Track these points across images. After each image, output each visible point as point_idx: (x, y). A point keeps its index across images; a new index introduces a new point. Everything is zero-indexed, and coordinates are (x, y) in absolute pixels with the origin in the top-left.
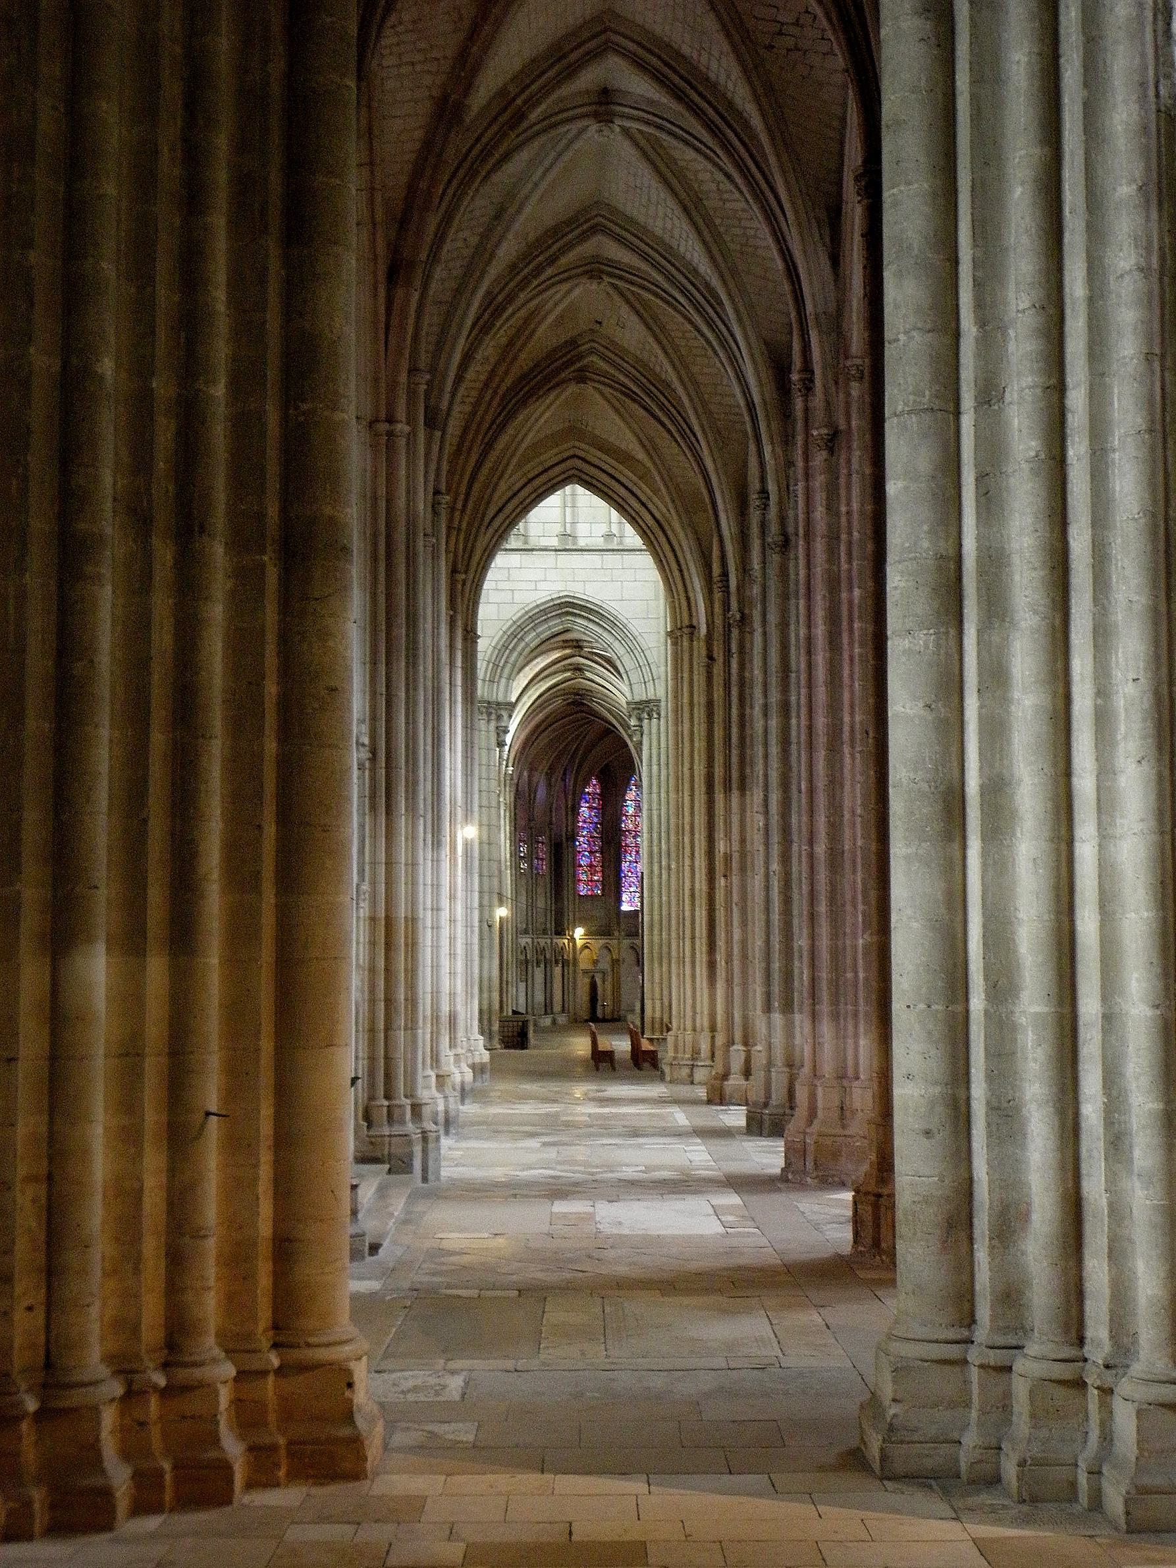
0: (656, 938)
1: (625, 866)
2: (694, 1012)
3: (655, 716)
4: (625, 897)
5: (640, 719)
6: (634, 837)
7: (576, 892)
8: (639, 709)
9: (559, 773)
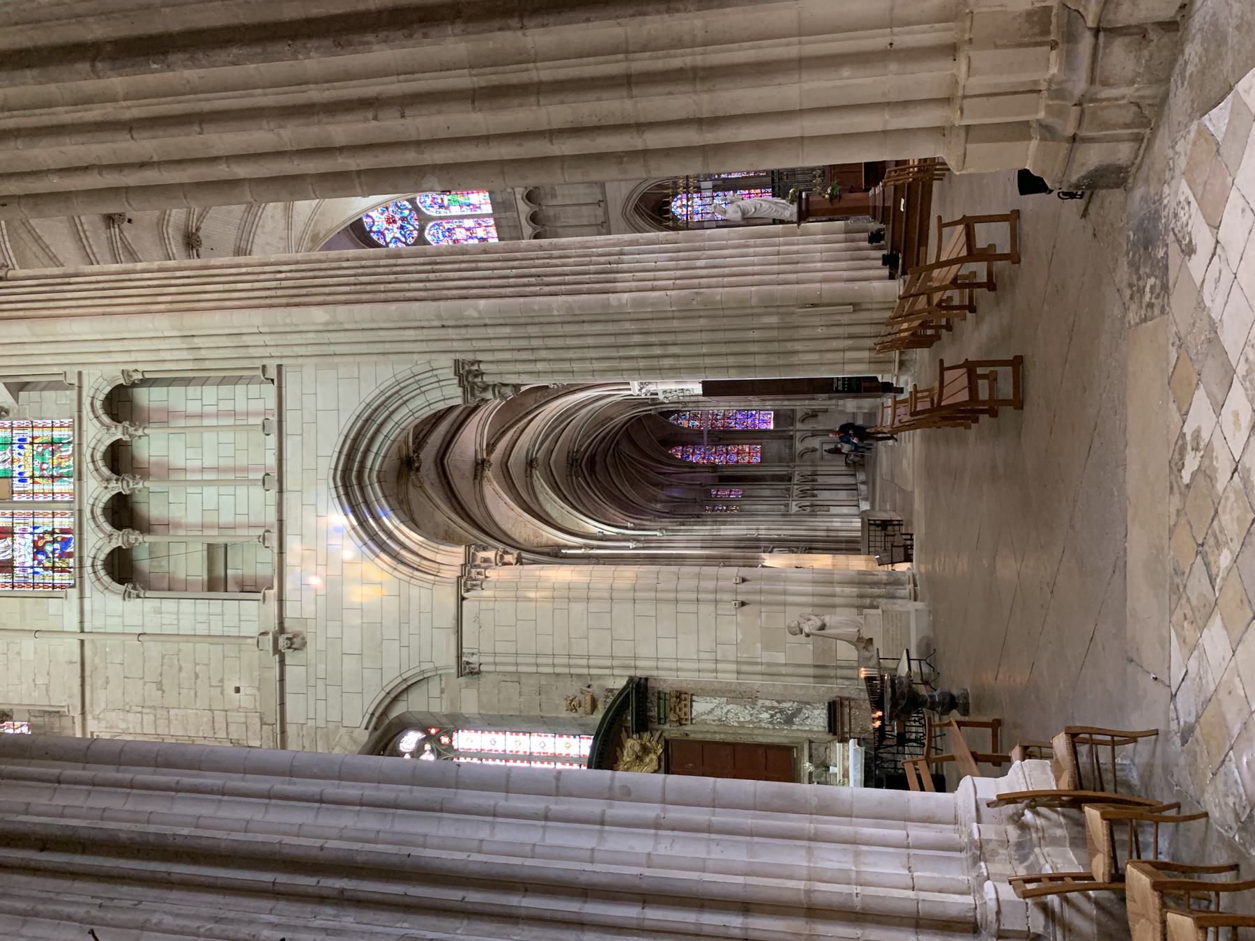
0: (759, 360)
1: (738, 428)
2: (890, 54)
3: (475, 367)
4: (764, 427)
5: (485, 388)
6: (717, 420)
7: (757, 466)
8: (472, 389)
9: (661, 478)
